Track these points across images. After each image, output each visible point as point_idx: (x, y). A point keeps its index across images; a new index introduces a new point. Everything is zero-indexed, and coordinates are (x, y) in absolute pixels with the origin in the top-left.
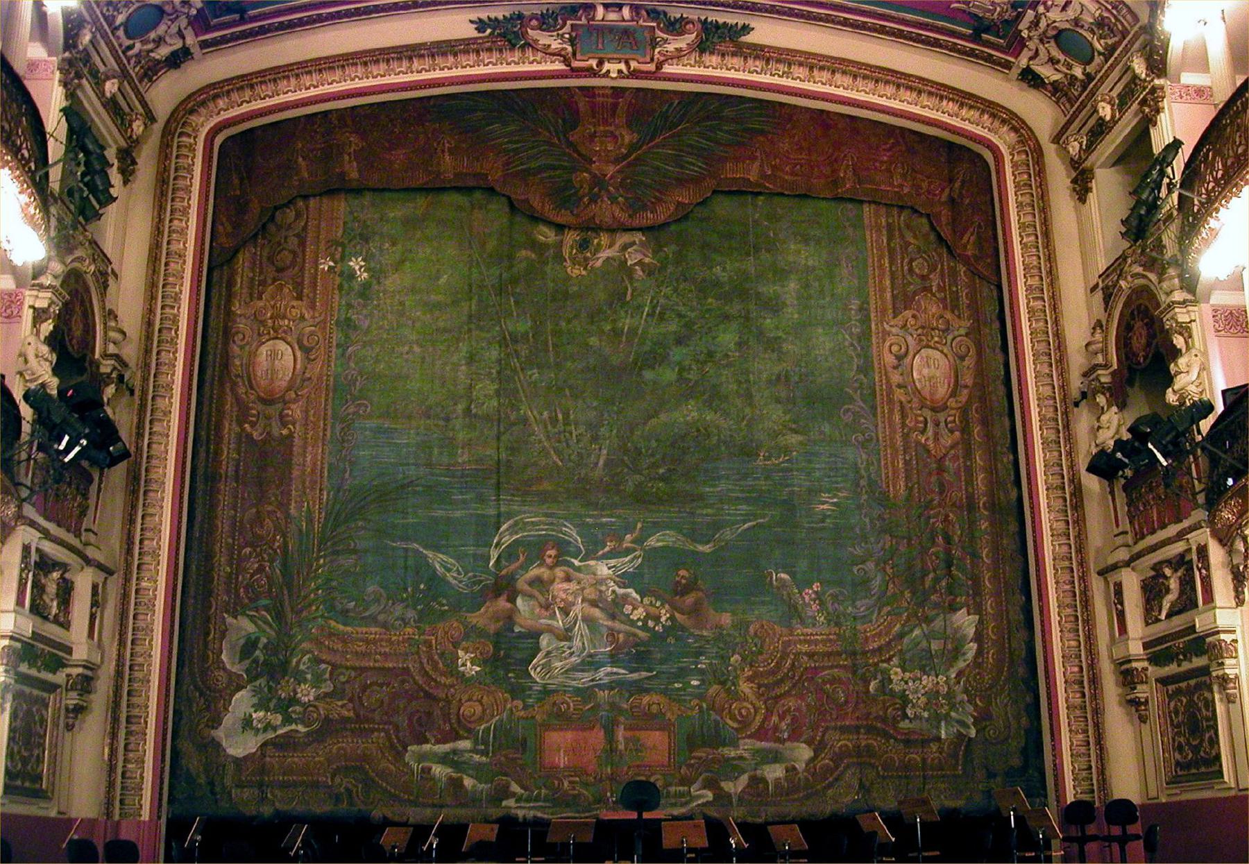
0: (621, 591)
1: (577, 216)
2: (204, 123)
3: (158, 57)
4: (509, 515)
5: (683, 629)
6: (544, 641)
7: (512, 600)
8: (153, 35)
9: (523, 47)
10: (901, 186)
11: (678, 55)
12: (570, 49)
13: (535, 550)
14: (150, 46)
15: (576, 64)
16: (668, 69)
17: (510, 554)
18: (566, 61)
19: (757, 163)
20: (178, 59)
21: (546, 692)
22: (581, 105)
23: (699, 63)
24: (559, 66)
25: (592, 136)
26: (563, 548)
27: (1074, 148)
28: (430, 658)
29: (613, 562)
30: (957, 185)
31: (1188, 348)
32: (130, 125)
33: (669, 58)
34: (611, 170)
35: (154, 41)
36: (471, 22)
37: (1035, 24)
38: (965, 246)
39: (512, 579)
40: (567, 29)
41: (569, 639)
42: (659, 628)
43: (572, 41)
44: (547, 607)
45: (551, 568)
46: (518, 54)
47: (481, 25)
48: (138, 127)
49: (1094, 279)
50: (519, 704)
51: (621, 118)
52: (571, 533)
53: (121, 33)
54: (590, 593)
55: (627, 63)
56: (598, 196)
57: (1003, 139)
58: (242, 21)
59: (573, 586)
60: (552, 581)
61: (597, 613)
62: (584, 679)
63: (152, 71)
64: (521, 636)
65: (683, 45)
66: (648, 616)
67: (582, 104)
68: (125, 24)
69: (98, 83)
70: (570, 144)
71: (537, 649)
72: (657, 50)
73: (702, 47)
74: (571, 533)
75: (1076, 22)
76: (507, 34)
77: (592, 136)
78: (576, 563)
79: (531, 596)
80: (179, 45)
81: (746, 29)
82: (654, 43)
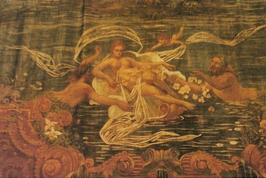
0: (171, 73)
4: (90, 25)
5: (220, 100)
6: (112, 112)
7: (89, 82)
13: (107, 47)
17: (89, 50)
21: (112, 152)
26: (128, 46)
28: (25, 126)
29: (163, 53)
39: (89, 67)
41: (131, 109)
42: (202, 100)
44: (114, 86)
45: (118, 58)
50: (91, 161)
52: (134, 35)
54: (148, 76)
59: (134, 71)
60: (118, 68)
61: (152, 89)
62: (143, 141)
64: (94, 108)
66: (192, 91)
71: (106, 118)
74: (134, 35)
78: (137, 55)
79: (104, 79)
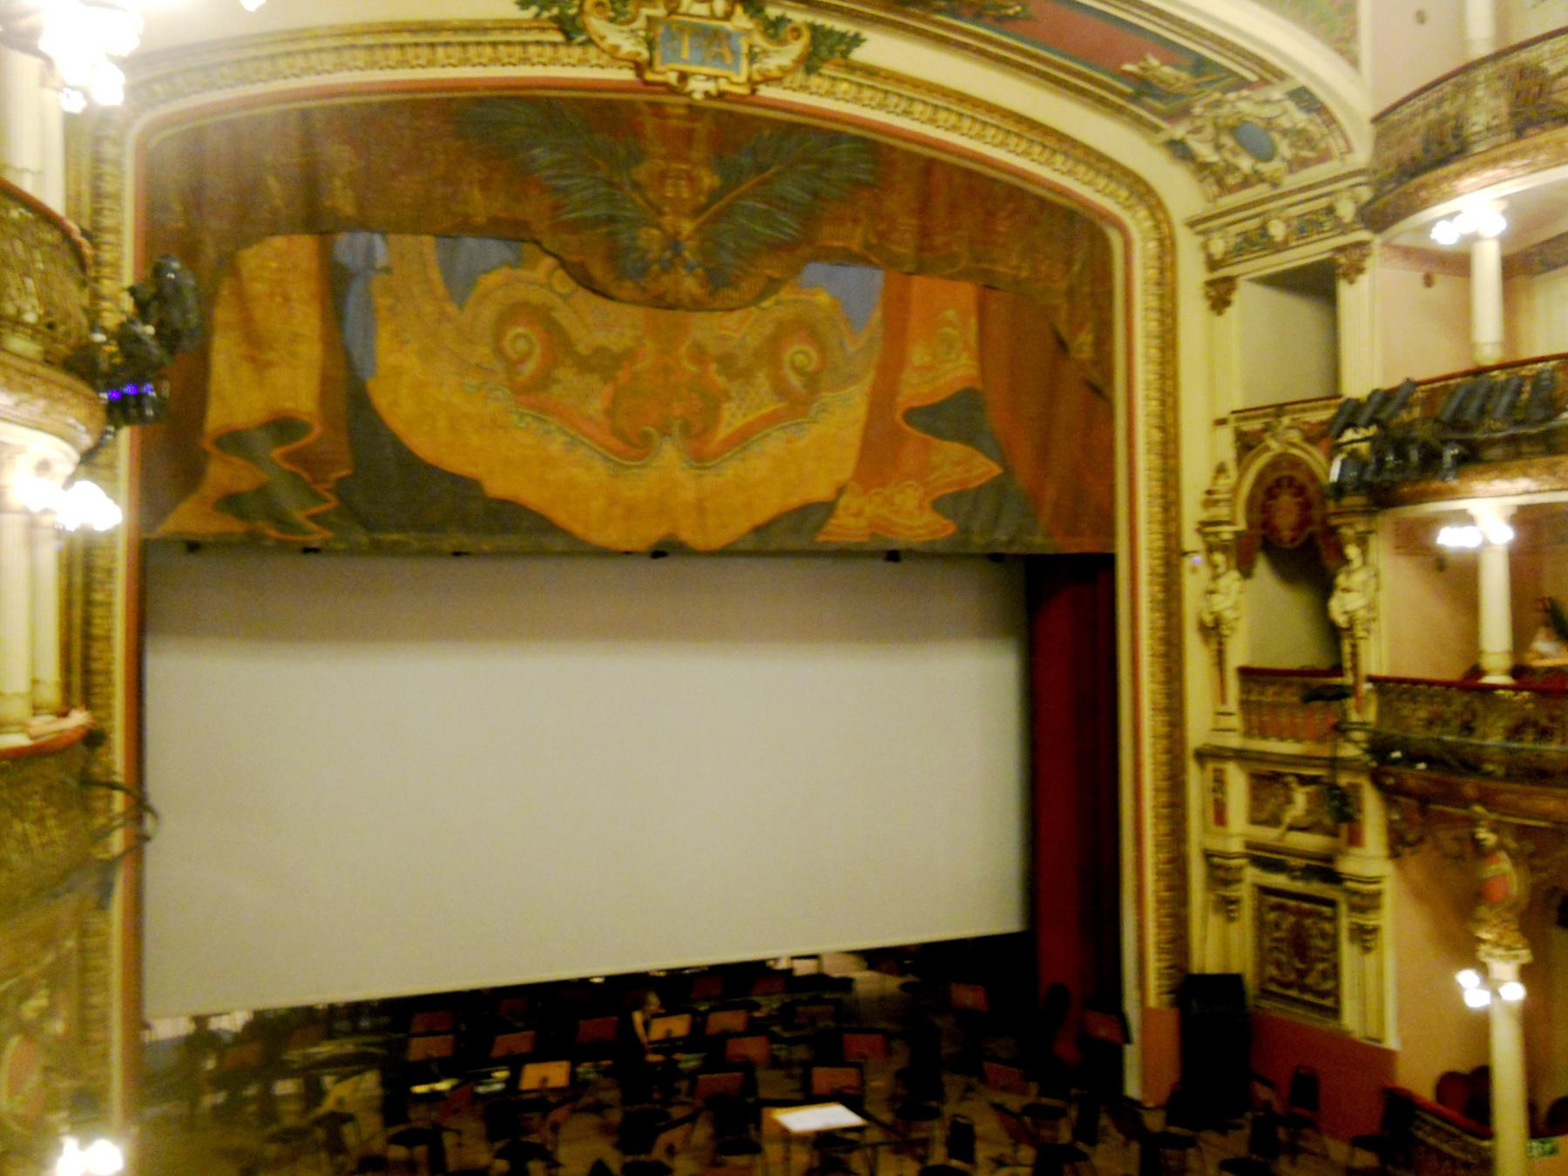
9: (582, 44)
10: (1018, 268)
12: (645, 54)
15: (649, 76)
16: (766, 92)
18: (639, 67)
23: (804, 88)
24: (627, 75)
25: (663, 176)
27: (1218, 247)
31: (1365, 563)
33: (768, 80)
34: (687, 227)
40: (640, 23)
43: (650, 44)
46: (577, 52)
49: (1222, 413)
51: (698, 153)
56: (671, 263)
57: (1137, 223)
67: (650, 125)
70: (636, 186)
73: (810, 63)
75: (1269, 121)
77: (663, 176)
81: (857, 40)
82: (752, 57)
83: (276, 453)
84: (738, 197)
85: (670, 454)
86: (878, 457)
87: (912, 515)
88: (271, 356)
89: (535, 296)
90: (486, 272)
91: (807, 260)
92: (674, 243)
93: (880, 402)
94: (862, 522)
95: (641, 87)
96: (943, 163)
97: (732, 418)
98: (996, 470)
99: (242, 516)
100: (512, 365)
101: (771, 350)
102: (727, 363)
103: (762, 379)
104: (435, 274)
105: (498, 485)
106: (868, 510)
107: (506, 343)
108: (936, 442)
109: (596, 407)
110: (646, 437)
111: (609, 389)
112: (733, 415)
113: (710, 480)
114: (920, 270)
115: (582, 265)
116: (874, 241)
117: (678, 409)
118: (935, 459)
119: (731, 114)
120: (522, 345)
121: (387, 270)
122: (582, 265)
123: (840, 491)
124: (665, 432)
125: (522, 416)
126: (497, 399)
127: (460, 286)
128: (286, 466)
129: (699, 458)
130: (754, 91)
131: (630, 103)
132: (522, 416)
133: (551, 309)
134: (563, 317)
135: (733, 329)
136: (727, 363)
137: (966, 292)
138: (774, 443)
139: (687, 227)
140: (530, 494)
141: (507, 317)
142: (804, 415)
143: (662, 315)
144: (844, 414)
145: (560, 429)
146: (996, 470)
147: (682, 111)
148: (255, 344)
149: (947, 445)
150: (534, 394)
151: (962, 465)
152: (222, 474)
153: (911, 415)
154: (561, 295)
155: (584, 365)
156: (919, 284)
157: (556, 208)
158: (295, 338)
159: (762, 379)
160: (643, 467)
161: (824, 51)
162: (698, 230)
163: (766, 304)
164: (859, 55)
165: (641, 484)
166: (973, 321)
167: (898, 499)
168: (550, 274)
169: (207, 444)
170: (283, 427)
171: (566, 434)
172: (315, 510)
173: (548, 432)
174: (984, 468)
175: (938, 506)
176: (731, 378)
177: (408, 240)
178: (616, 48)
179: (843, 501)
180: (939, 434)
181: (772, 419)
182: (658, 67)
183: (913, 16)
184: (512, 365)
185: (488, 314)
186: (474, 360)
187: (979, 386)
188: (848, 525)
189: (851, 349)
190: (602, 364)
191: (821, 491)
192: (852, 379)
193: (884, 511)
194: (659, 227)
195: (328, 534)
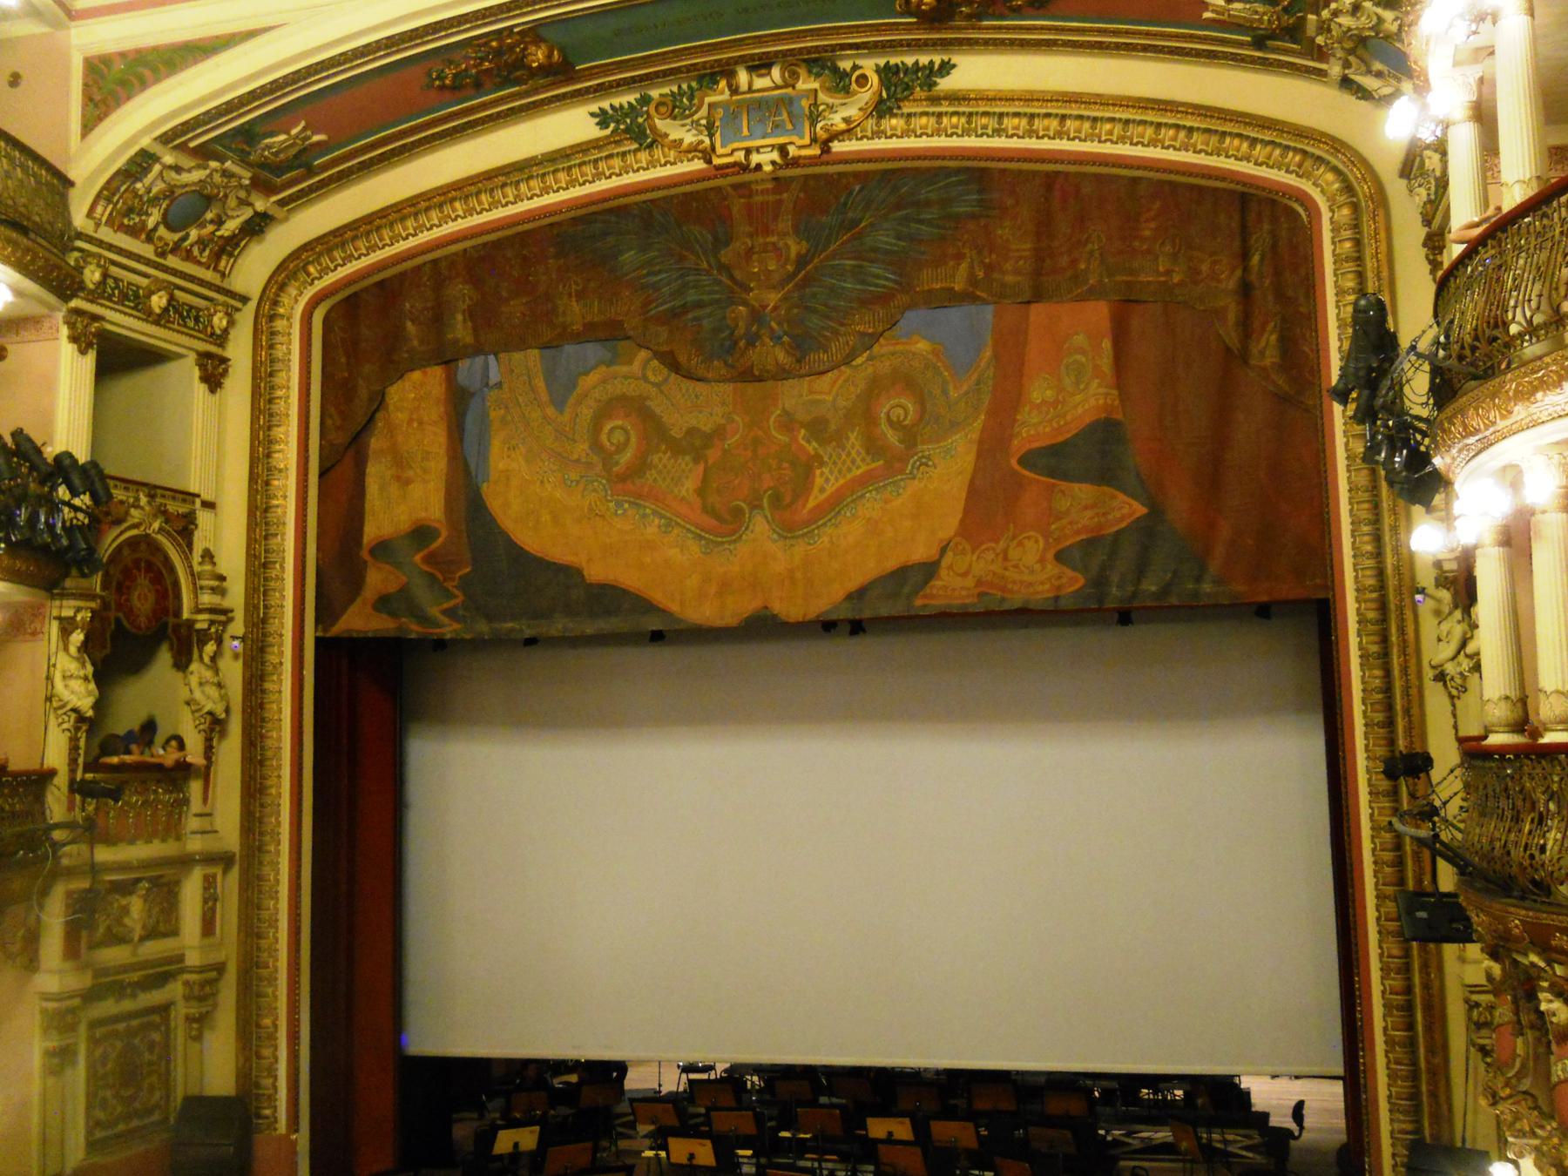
1: (733, 367)
2: (295, 302)
3: (227, 234)
8: (209, 216)
11: (848, 133)
12: (707, 141)
14: (211, 228)
15: (716, 161)
18: (707, 156)
19: (964, 265)
20: (257, 226)
22: (735, 210)
23: (878, 134)
24: (698, 165)
25: (750, 252)
30: (1256, 259)
32: (210, 321)
34: (772, 298)
35: (212, 222)
36: (593, 115)
37: (1324, 28)
38: (1262, 353)
40: (704, 111)
43: (710, 128)
47: (603, 119)
48: (219, 321)
51: (785, 223)
53: (162, 231)
55: (782, 149)
56: (757, 336)
57: (1319, 190)
58: (311, 171)
63: (228, 248)
65: (852, 112)
67: (737, 206)
68: (166, 221)
69: (135, 300)
70: (723, 268)
72: (819, 125)
73: (881, 109)
76: (632, 131)
77: (750, 252)
80: (248, 213)
81: (946, 68)
83: (418, 558)
84: (827, 258)
85: (760, 526)
86: (988, 508)
87: (1031, 568)
88: (410, 473)
89: (631, 388)
90: (586, 373)
91: (909, 307)
92: (757, 315)
93: (991, 447)
94: (970, 582)
95: (714, 172)
96: (1067, 175)
97: (826, 483)
98: (1140, 510)
99: (393, 614)
100: (608, 459)
101: (864, 413)
102: (817, 428)
103: (854, 439)
104: (540, 383)
105: (596, 572)
106: (980, 568)
107: (604, 437)
108: (1063, 485)
109: (689, 486)
110: (737, 513)
111: (701, 467)
112: (827, 480)
113: (800, 549)
114: (1038, 296)
115: (672, 353)
116: (981, 274)
117: (768, 481)
118: (1063, 504)
119: (816, 177)
120: (618, 437)
121: (499, 385)
122: (672, 353)
123: (943, 551)
124: (755, 506)
125: (619, 504)
126: (595, 490)
127: (561, 390)
128: (425, 568)
129: (789, 529)
130: (826, 149)
131: (718, 190)
132: (619, 504)
133: (647, 398)
134: (657, 405)
135: (829, 392)
136: (817, 428)
137: (1098, 313)
138: (871, 505)
139: (772, 298)
140: (629, 578)
141: (605, 411)
142: (902, 471)
143: (751, 389)
144: (949, 468)
145: (655, 513)
146: (1140, 510)
147: (770, 186)
148: (400, 462)
149: (1076, 486)
150: (627, 482)
151: (1090, 508)
152: (377, 579)
153: (1027, 460)
154: (654, 384)
155: (677, 449)
156: (1038, 312)
157: (646, 304)
158: (427, 456)
159: (854, 439)
160: (735, 541)
161: (898, 88)
162: (785, 299)
163: (859, 360)
164: (945, 84)
165: (735, 560)
166: (1107, 344)
167: (1014, 554)
168: (645, 364)
169: (365, 554)
170: (421, 534)
171: (662, 517)
172: (445, 606)
173: (644, 516)
174: (1127, 509)
175: (1060, 557)
176: (824, 442)
177: (517, 356)
178: (681, 141)
179: (945, 562)
180: (1065, 477)
181: (864, 481)
182: (719, 150)
183: (959, 29)
184: (608, 459)
185: (586, 413)
186: (575, 457)
187: (1120, 417)
188: (954, 586)
189: (953, 394)
190: (695, 444)
191: (921, 552)
192: (955, 426)
193: (997, 568)
194: (745, 303)
195: (456, 626)
